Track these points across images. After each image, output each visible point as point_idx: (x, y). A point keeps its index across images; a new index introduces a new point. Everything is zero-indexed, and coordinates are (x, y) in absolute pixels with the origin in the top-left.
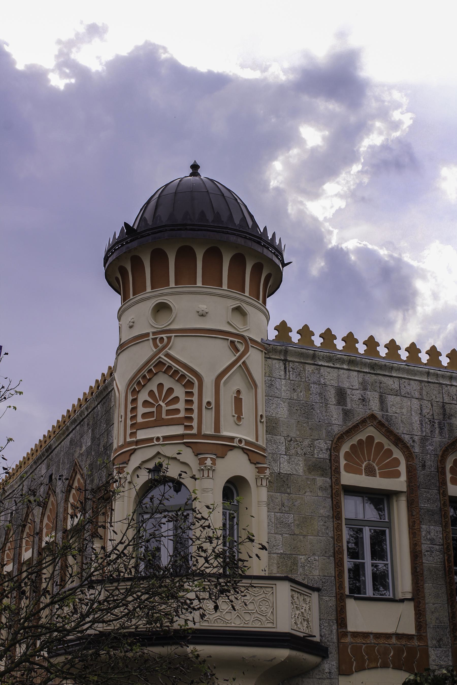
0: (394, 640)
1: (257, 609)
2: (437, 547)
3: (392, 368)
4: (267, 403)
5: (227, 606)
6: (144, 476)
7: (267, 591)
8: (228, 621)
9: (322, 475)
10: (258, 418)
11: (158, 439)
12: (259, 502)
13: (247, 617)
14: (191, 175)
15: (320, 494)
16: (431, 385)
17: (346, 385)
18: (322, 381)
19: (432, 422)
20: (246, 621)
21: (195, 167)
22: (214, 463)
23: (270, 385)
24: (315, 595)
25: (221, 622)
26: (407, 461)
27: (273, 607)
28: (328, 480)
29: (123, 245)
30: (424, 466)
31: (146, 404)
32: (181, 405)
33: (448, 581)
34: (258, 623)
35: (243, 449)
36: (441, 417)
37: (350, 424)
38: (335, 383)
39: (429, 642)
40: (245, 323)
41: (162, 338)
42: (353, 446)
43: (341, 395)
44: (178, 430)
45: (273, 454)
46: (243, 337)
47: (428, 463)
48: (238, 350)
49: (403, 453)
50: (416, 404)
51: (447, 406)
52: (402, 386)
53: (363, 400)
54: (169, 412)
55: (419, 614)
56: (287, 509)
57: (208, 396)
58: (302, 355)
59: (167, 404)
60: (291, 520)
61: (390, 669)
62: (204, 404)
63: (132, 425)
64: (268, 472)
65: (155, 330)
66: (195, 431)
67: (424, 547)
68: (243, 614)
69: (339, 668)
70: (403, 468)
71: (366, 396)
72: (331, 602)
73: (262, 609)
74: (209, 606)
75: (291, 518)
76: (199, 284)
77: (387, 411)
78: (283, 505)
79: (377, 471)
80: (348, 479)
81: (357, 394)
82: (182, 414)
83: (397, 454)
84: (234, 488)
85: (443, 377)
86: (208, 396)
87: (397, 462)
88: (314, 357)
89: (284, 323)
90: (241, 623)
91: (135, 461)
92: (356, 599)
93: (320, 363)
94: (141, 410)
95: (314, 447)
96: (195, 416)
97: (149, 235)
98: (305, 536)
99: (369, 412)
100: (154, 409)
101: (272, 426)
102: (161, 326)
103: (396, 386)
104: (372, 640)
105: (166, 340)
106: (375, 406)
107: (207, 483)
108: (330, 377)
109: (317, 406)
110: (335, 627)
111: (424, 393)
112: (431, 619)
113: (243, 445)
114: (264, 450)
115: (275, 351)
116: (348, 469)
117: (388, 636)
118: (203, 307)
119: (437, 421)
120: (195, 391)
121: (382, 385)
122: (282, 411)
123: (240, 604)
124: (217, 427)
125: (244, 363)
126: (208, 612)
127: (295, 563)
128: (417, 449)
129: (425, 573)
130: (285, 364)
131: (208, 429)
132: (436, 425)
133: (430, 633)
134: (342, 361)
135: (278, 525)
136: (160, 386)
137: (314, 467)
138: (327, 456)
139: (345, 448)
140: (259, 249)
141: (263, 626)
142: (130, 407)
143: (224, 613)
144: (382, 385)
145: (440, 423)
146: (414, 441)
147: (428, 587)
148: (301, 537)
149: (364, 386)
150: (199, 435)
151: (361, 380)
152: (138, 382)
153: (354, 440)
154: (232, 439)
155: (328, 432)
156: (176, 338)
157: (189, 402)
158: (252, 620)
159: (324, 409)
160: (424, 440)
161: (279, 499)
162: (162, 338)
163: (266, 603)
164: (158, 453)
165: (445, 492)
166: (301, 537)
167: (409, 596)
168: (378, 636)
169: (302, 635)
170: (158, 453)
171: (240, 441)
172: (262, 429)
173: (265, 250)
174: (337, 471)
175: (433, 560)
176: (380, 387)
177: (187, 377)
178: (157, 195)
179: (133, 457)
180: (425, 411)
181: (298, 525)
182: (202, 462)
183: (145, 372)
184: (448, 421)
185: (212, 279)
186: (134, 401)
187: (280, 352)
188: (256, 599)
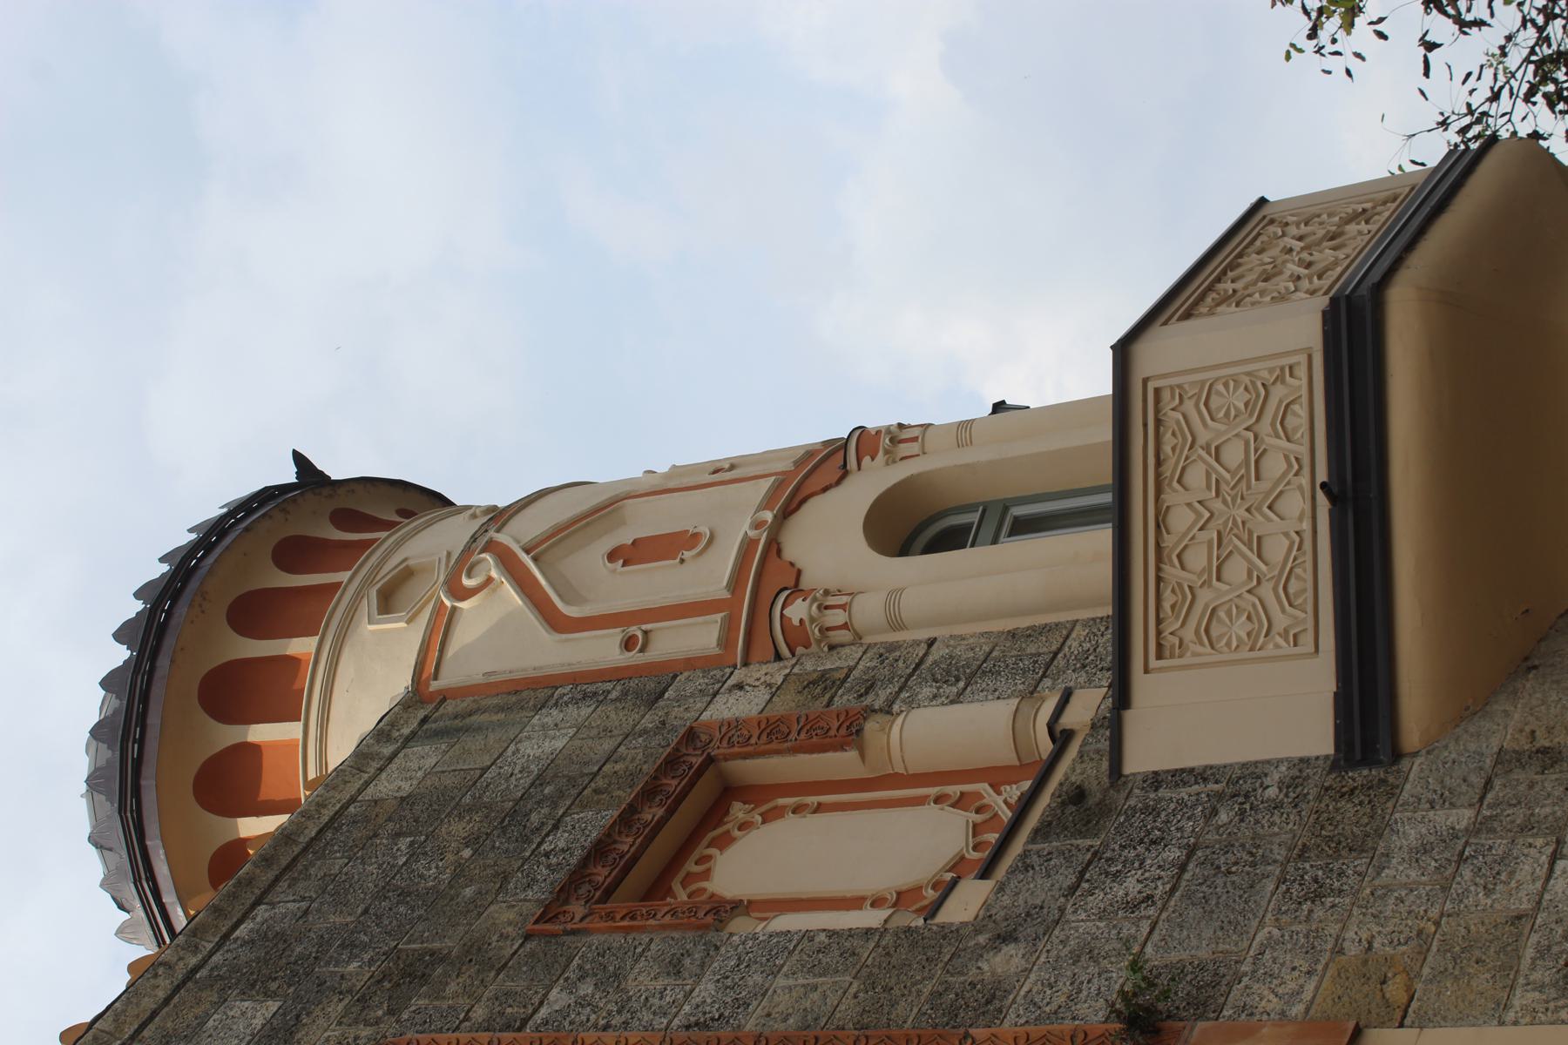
1: (1240, 429)
5: (1236, 556)
7: (1173, 397)
8: (1292, 543)
13: (1274, 466)
20: (1290, 465)
25: (1298, 578)
34: (1295, 414)
68: (1265, 485)
73: (1242, 406)
74: (1239, 638)
90: (1300, 488)
123: (1225, 502)
126: (1262, 639)
141: (1304, 392)
143: (1263, 567)
158: (1283, 443)
163: (1219, 394)
188: (1203, 436)
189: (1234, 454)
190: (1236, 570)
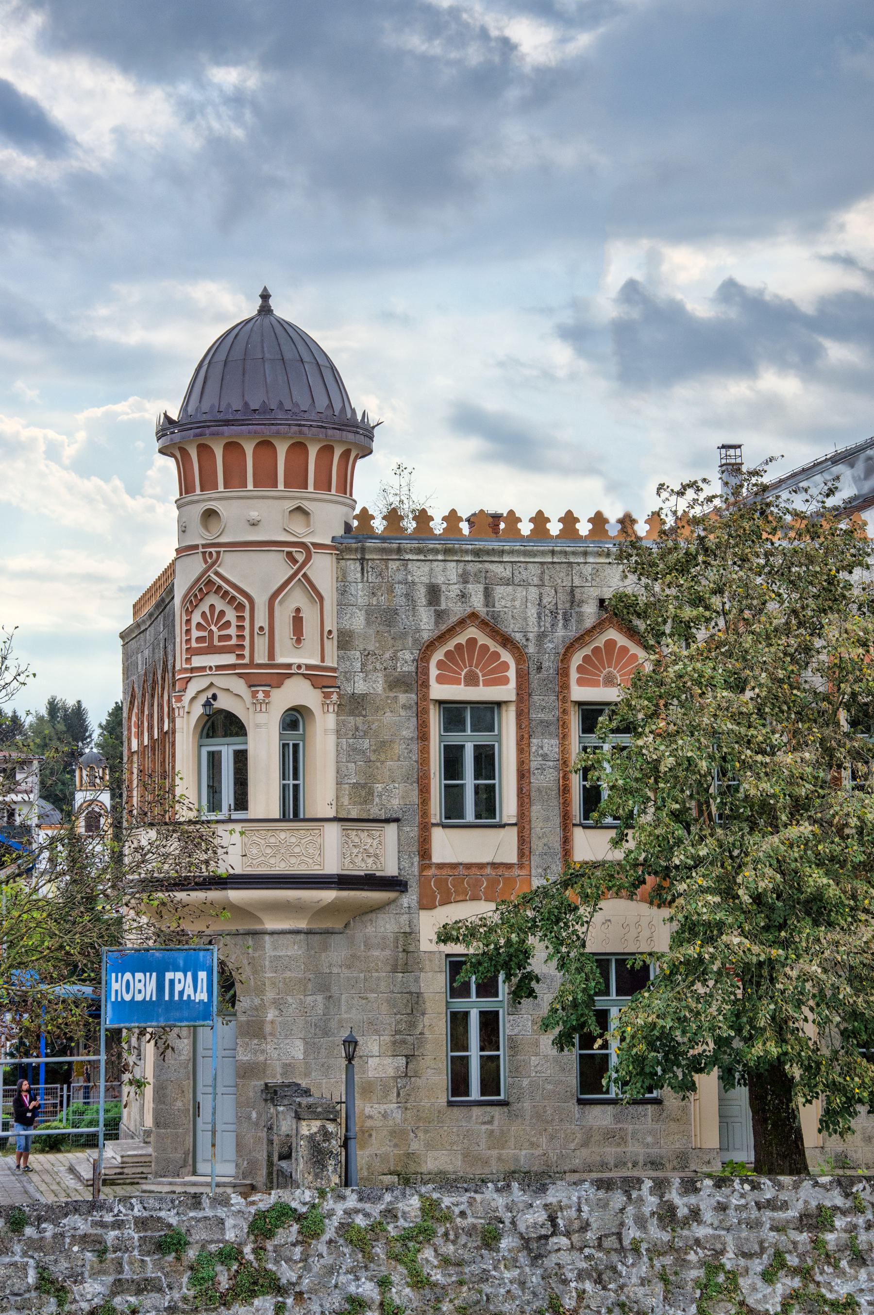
0: (488, 870)
2: (551, 764)
3: (502, 552)
4: (340, 614)
6: (198, 710)
9: (406, 692)
10: (324, 635)
11: (211, 668)
12: (325, 730)
13: (293, 860)
14: (260, 311)
15: (403, 713)
16: (557, 566)
17: (440, 580)
18: (410, 578)
19: (554, 614)
21: (265, 296)
22: (267, 694)
23: (343, 592)
24: (393, 827)
26: (517, 664)
27: (321, 848)
28: (414, 696)
29: (166, 435)
30: (539, 669)
31: (199, 624)
32: (232, 631)
33: (562, 801)
35: (303, 675)
36: (568, 605)
37: (443, 628)
38: (425, 579)
39: (533, 871)
40: (308, 525)
41: (211, 553)
42: (448, 654)
43: (434, 593)
44: (229, 659)
45: (346, 673)
46: (302, 545)
47: (546, 665)
48: (295, 561)
49: (513, 655)
50: (533, 592)
51: (577, 591)
52: (516, 573)
53: (463, 596)
54: (222, 638)
55: (523, 841)
56: (362, 734)
57: (261, 619)
58: (383, 550)
59: (220, 629)
60: (366, 745)
61: (482, 902)
62: (256, 630)
63: (187, 649)
64: (335, 697)
65: (204, 542)
66: (246, 661)
67: (533, 765)
69: (419, 902)
70: (512, 674)
71: (466, 591)
72: (412, 831)
75: (366, 744)
76: (250, 487)
77: (494, 606)
78: (357, 729)
79: (481, 679)
80: (439, 691)
81: (455, 590)
82: (234, 641)
83: (506, 656)
84: (295, 719)
85: (574, 553)
86: (261, 619)
87: (505, 666)
88: (399, 551)
89: (364, 510)
91: (193, 688)
92: (444, 826)
93: (407, 557)
94: (195, 634)
95: (397, 659)
96: (247, 643)
97: (191, 429)
98: (383, 763)
99: (469, 610)
100: (206, 634)
101: (345, 640)
102: (209, 538)
103: (508, 574)
104: (462, 871)
105: (214, 554)
106: (477, 602)
107: (261, 718)
108: (420, 573)
109: (401, 611)
110: (416, 859)
111: (547, 577)
112: (537, 845)
113: (303, 671)
114: (334, 670)
115: (349, 550)
116: (440, 680)
117: (481, 866)
118: (254, 515)
119: (560, 612)
120: (247, 615)
121: (488, 575)
122: (357, 622)
124: (271, 655)
125: (305, 575)
127: (371, 793)
128: (531, 649)
129: (533, 794)
130: (362, 564)
131: (261, 658)
132: (560, 617)
133: (535, 860)
134: (436, 552)
135: (348, 753)
136: (212, 607)
137: (396, 683)
138: (413, 669)
139: (439, 655)
140: (321, 434)
142: (184, 628)
144: (488, 575)
145: (565, 614)
146: (527, 640)
147: (536, 810)
148: (379, 764)
149: (464, 578)
150: (252, 664)
151: (460, 571)
152: (193, 600)
153: (450, 645)
154: (289, 666)
155: (415, 641)
156: (227, 554)
157: (240, 628)
159: (411, 613)
160: (541, 636)
161: (353, 724)
162: (211, 553)
164: (212, 684)
165: (565, 700)
166: (379, 764)
167: (514, 821)
168: (468, 866)
169: (362, 873)
170: (212, 684)
171: (299, 667)
172: (331, 647)
173: (330, 432)
174: (426, 685)
175: (544, 779)
176: (486, 578)
177: (240, 600)
178: (207, 362)
179: (189, 685)
180: (545, 601)
181: (375, 751)
182: (254, 695)
183: (195, 590)
184: (577, 609)
185: (266, 479)
186: (188, 621)
187: (356, 550)
189: (297, 850)
190: (269, 851)
